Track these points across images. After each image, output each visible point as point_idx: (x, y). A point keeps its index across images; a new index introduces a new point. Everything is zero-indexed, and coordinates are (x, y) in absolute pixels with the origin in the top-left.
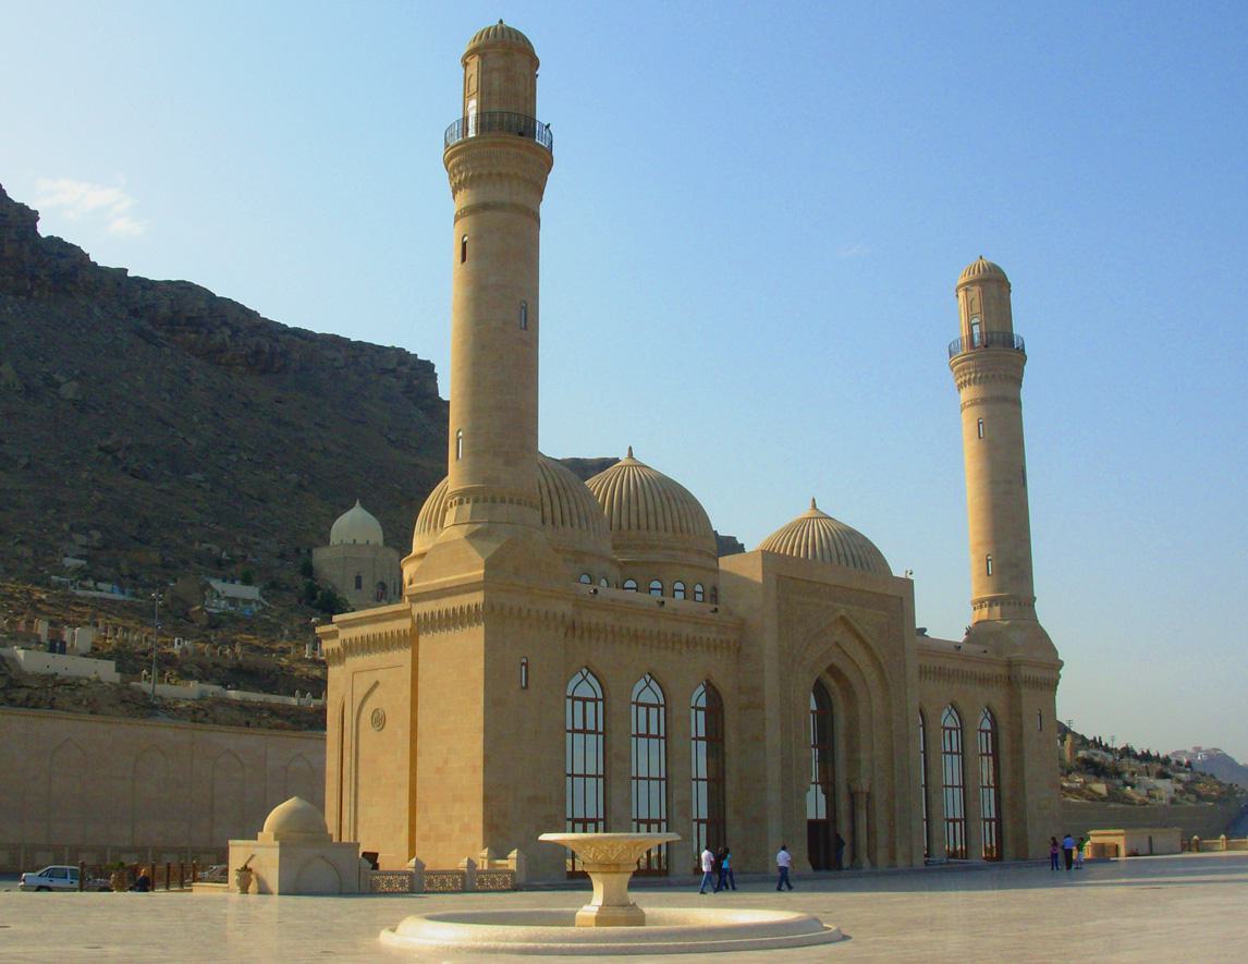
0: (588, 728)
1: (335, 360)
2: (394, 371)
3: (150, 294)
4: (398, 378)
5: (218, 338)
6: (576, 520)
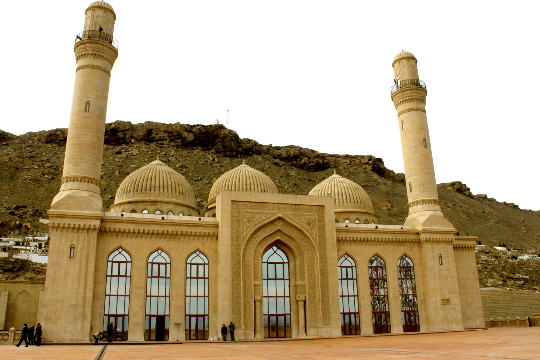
0: (199, 276)
2: (368, 163)
3: (280, 151)
4: (369, 165)
5: (303, 161)
6: (157, 189)
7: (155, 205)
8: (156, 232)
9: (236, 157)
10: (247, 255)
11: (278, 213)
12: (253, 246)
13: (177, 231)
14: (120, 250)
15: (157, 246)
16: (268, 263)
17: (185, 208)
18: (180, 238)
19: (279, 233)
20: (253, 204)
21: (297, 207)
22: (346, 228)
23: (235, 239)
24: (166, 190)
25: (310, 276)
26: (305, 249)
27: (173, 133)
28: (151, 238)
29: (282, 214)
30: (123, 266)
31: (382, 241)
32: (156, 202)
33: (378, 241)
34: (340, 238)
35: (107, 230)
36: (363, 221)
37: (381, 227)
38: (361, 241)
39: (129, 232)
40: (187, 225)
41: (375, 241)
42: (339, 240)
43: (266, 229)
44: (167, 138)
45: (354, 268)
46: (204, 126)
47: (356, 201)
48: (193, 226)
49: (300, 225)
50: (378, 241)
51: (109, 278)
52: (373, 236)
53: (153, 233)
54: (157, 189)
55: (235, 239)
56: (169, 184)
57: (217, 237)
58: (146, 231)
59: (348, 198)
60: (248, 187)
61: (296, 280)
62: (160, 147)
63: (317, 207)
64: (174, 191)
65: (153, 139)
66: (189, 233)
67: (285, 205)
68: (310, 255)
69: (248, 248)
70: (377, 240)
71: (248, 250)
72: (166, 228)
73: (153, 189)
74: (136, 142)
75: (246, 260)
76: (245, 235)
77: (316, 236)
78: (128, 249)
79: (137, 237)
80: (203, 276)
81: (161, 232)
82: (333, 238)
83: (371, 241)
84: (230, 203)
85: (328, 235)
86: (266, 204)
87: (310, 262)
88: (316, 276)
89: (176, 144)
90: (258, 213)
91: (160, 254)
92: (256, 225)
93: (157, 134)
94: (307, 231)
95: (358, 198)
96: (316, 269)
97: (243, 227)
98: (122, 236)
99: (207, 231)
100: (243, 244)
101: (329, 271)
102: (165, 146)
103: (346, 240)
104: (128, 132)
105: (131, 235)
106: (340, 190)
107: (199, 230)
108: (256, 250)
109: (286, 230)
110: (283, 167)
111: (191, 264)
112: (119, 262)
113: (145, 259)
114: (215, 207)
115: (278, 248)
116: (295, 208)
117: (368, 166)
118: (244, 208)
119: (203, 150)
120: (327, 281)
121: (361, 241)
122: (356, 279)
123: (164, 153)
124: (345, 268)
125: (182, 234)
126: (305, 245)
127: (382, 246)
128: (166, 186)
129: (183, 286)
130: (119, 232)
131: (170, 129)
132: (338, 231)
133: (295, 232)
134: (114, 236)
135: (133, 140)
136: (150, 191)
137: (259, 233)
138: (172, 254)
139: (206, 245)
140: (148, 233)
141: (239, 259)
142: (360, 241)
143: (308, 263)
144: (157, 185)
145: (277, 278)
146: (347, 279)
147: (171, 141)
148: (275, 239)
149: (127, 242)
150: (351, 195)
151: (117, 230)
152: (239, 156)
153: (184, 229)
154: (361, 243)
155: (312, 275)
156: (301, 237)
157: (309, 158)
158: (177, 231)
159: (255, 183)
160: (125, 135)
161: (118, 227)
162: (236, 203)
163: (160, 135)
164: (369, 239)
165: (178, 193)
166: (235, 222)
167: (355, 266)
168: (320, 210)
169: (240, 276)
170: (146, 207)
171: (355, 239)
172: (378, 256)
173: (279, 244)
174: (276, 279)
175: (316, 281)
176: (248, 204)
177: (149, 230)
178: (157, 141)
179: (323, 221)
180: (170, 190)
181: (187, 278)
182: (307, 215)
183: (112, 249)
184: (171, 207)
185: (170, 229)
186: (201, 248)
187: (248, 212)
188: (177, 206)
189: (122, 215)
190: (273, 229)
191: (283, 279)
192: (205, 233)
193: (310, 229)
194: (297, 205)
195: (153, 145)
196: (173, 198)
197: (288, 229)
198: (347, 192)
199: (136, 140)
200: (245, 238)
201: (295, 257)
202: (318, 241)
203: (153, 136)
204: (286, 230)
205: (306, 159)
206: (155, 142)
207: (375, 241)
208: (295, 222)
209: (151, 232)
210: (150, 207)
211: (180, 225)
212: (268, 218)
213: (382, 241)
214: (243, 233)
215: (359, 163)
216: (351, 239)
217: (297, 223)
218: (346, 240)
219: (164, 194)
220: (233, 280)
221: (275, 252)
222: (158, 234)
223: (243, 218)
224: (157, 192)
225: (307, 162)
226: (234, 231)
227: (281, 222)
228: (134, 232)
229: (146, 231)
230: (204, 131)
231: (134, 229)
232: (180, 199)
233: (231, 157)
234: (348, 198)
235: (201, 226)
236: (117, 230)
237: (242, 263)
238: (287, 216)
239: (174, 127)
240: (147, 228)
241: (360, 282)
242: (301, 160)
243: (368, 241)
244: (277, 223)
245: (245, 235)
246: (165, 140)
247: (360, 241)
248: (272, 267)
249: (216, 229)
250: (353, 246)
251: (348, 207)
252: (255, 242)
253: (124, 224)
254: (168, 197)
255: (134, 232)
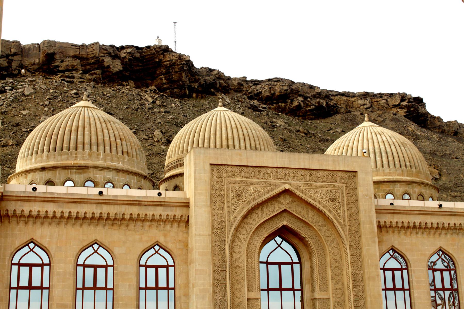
1: (364, 105)
2: (399, 105)
3: (258, 87)
4: (401, 108)
5: (296, 104)
6: (87, 146)
7: (84, 172)
8: (89, 215)
9: (190, 97)
10: (236, 250)
11: (284, 184)
12: (244, 237)
13: (124, 214)
14: (32, 245)
15: (92, 238)
16: (268, 263)
17: (132, 176)
18: (128, 226)
19: (285, 215)
20: (243, 169)
21: (313, 173)
22: (391, 207)
23: (216, 225)
24: (101, 148)
25: (337, 283)
26: (327, 241)
27: (88, 59)
28: (81, 225)
29: (290, 184)
30: (36, 271)
31: (449, 228)
32: (87, 167)
33: (443, 228)
34: (382, 224)
35: (11, 213)
36: (415, 195)
37: (447, 205)
38: (415, 228)
39: (46, 217)
40: (139, 203)
41: (437, 228)
42: (379, 227)
43: (265, 209)
44: (79, 67)
45: (405, 272)
46: (137, 48)
47: (403, 163)
48: (149, 205)
49: (320, 203)
50: (443, 228)
51: (13, 292)
52: (434, 220)
53: (85, 218)
54: (87, 146)
55: (217, 224)
56: (107, 138)
57: (187, 222)
58: (74, 215)
59: (391, 159)
60: (231, 142)
61: (313, 291)
62: (67, 82)
63: (344, 174)
64: (114, 149)
65: (56, 70)
66: (142, 217)
67: (294, 171)
68: (335, 250)
69: (237, 240)
70: (441, 226)
71: (237, 242)
72: (105, 209)
73: (80, 147)
74: (28, 74)
75: (234, 259)
76: (231, 218)
77: (344, 220)
78: (45, 243)
79: (59, 224)
80: (165, 285)
81: (97, 215)
82: (371, 223)
83: (432, 228)
84: (208, 167)
85: (363, 217)
86: (264, 169)
87: (336, 261)
88: (346, 283)
89: (94, 76)
90: (251, 183)
91: (96, 252)
92: (249, 203)
93: (62, 61)
94: (330, 211)
95: (407, 159)
96: (345, 273)
97: (228, 206)
98: (35, 223)
99: (171, 212)
100: (229, 232)
101: (366, 276)
102: (75, 80)
103: (391, 226)
104: (15, 58)
105: (41, 220)
106: (376, 146)
107: (158, 211)
108: (249, 243)
109: (297, 210)
110: (264, 113)
111: (147, 266)
112: (31, 266)
113: (72, 259)
114: (182, 175)
115: (284, 239)
116: (311, 175)
117: (399, 110)
118: (229, 176)
119: (137, 87)
120: (363, 292)
121: (415, 228)
122: (409, 290)
123: (74, 91)
124: (390, 272)
125: (131, 219)
126: (328, 234)
127: (449, 236)
128: (100, 141)
129: (135, 303)
130: (30, 216)
131: (83, 53)
132: (380, 211)
133: (311, 213)
134: (22, 224)
135: (23, 71)
136: (76, 150)
137: (254, 216)
138: (116, 251)
139: (170, 236)
140: (77, 218)
141: (224, 257)
142: (414, 227)
143: (331, 263)
144: (87, 140)
145: (283, 287)
146: (394, 289)
147: (85, 72)
148: (279, 225)
149: (42, 233)
150: (395, 154)
151: (26, 213)
152: (194, 95)
153: (135, 210)
154: (414, 232)
155: (338, 281)
156: (321, 221)
157: (306, 98)
158: (124, 214)
159: (241, 136)
160: (10, 62)
161: (27, 208)
162: (217, 167)
163: (67, 63)
164: (429, 225)
165: (120, 153)
166: (217, 198)
167: (407, 269)
168: (349, 178)
169: (226, 285)
170: (69, 175)
171: (406, 224)
172: (444, 253)
173: (285, 233)
174: (281, 289)
175: (346, 293)
176: (236, 169)
177: (78, 213)
178: (63, 72)
179: (356, 195)
180: (108, 148)
181: (140, 289)
182: (330, 187)
183: (18, 244)
184: (110, 175)
185: (113, 210)
186: (162, 240)
187: (236, 183)
188: (121, 174)
189: (34, 189)
190: (277, 208)
191: (293, 289)
192: (168, 215)
193: (335, 208)
194: (314, 170)
195: (57, 79)
196: (113, 161)
197: (300, 209)
198: (389, 150)
199: (29, 71)
200: (232, 224)
201: (310, 254)
202: (347, 227)
203: (57, 64)
204: (297, 210)
205: (301, 99)
206: (60, 75)
207: (437, 228)
208: (310, 197)
209: (82, 215)
210: (77, 175)
211: (127, 204)
212: (268, 192)
213: (449, 228)
214: (229, 216)
215: (386, 105)
216: (400, 225)
217: (314, 199)
218: (391, 226)
219: (99, 155)
220: (214, 292)
221: (279, 246)
222: (93, 218)
223: (228, 191)
224: (87, 151)
225: (302, 104)
226: (215, 212)
227: (288, 197)
228: (54, 217)
229: (74, 215)
230: (138, 55)
231: (54, 212)
232: (123, 163)
233: (182, 97)
234: (391, 159)
235: (161, 205)
236: (26, 213)
237: (228, 263)
238: (297, 189)
239: (90, 50)
240: (75, 209)
241: (416, 294)
242: (292, 101)
243: (426, 228)
244: (282, 199)
245: (231, 218)
246: (77, 70)
247: (414, 227)
248: (274, 269)
249: (185, 209)
250: (403, 236)
251: (390, 174)
252: (248, 229)
253: (37, 203)
254: (105, 160)
255: (54, 217)
